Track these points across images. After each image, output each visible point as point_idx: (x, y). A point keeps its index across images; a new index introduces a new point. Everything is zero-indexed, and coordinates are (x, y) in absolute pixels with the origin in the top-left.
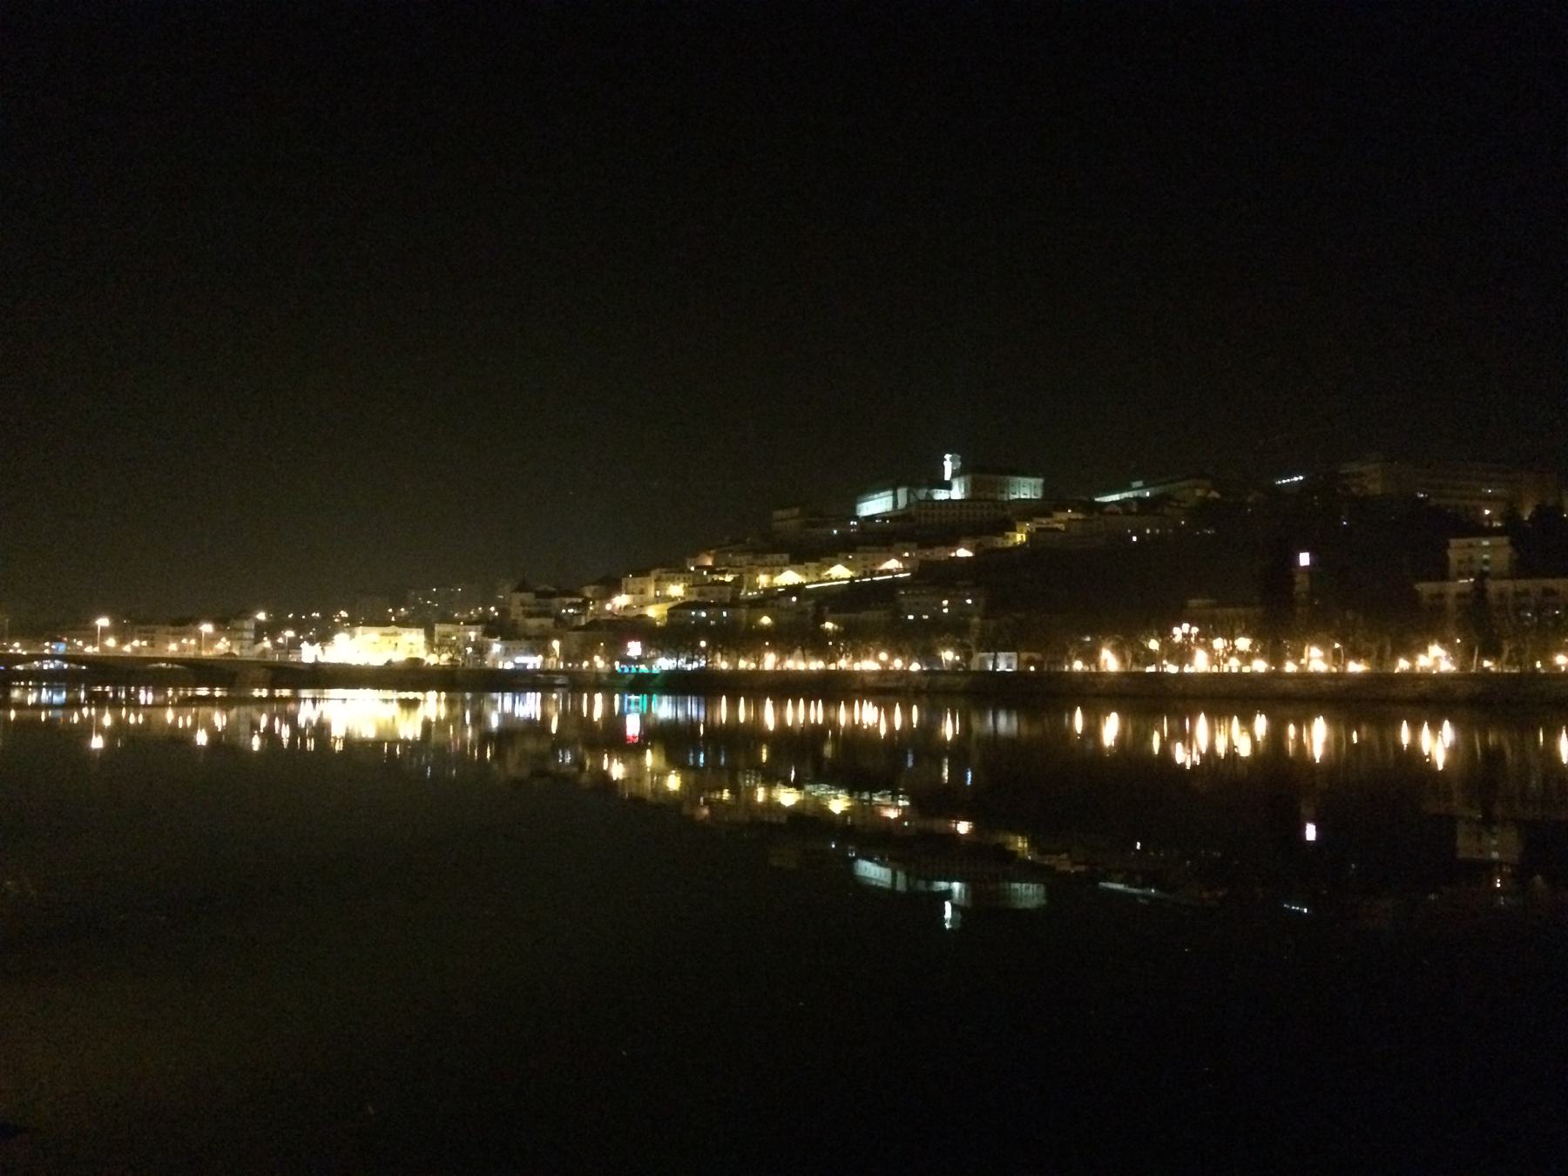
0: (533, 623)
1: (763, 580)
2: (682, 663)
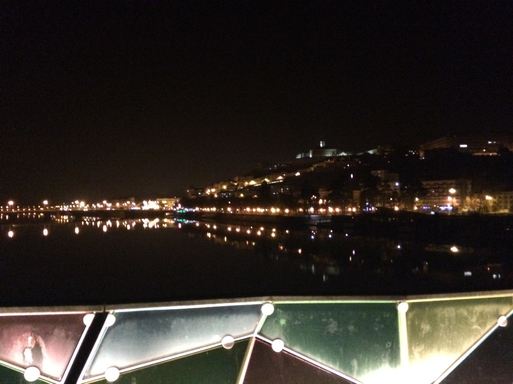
1: (246, 183)
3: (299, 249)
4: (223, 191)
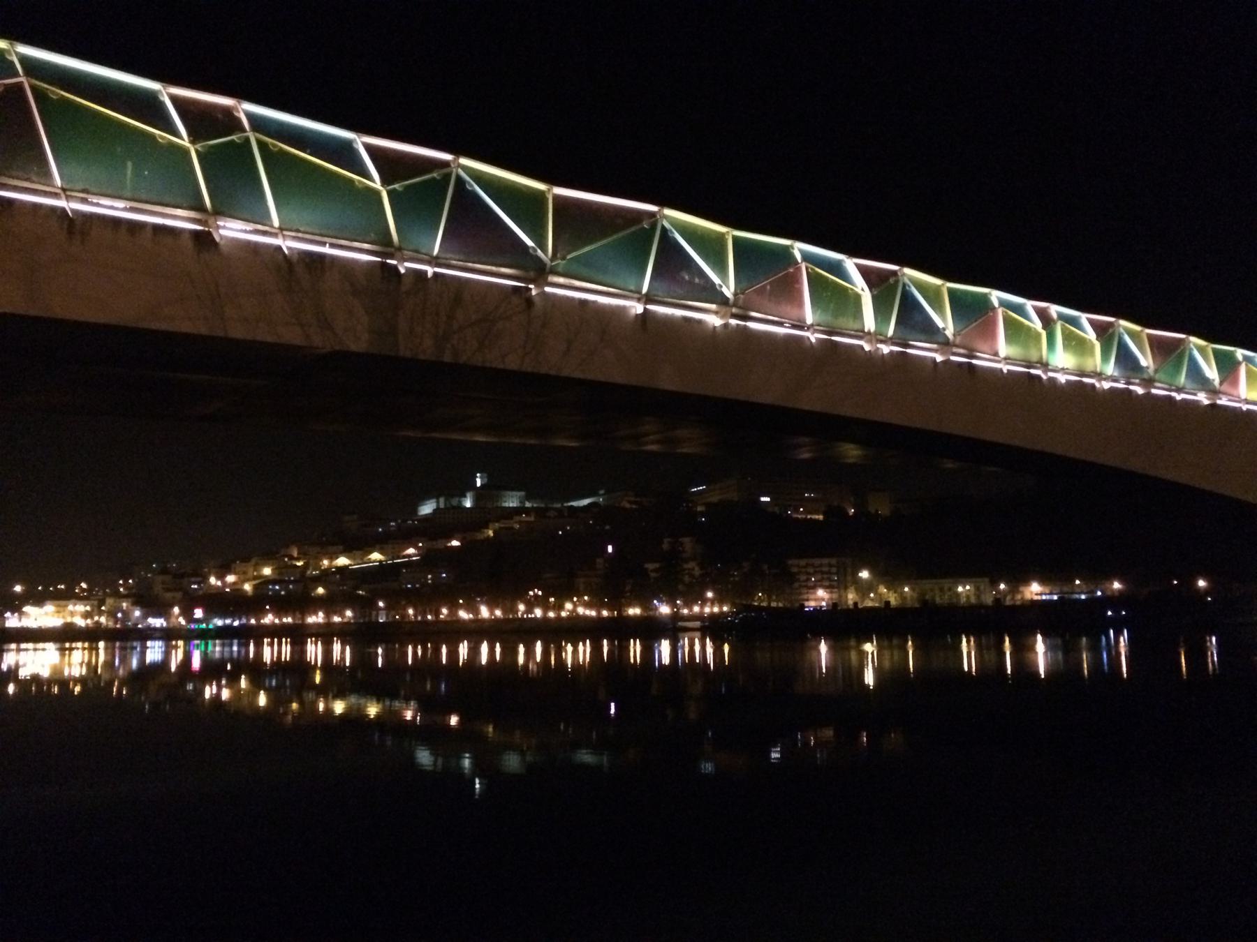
0: (169, 595)
2: (244, 621)
3: (450, 714)
4: (267, 581)
